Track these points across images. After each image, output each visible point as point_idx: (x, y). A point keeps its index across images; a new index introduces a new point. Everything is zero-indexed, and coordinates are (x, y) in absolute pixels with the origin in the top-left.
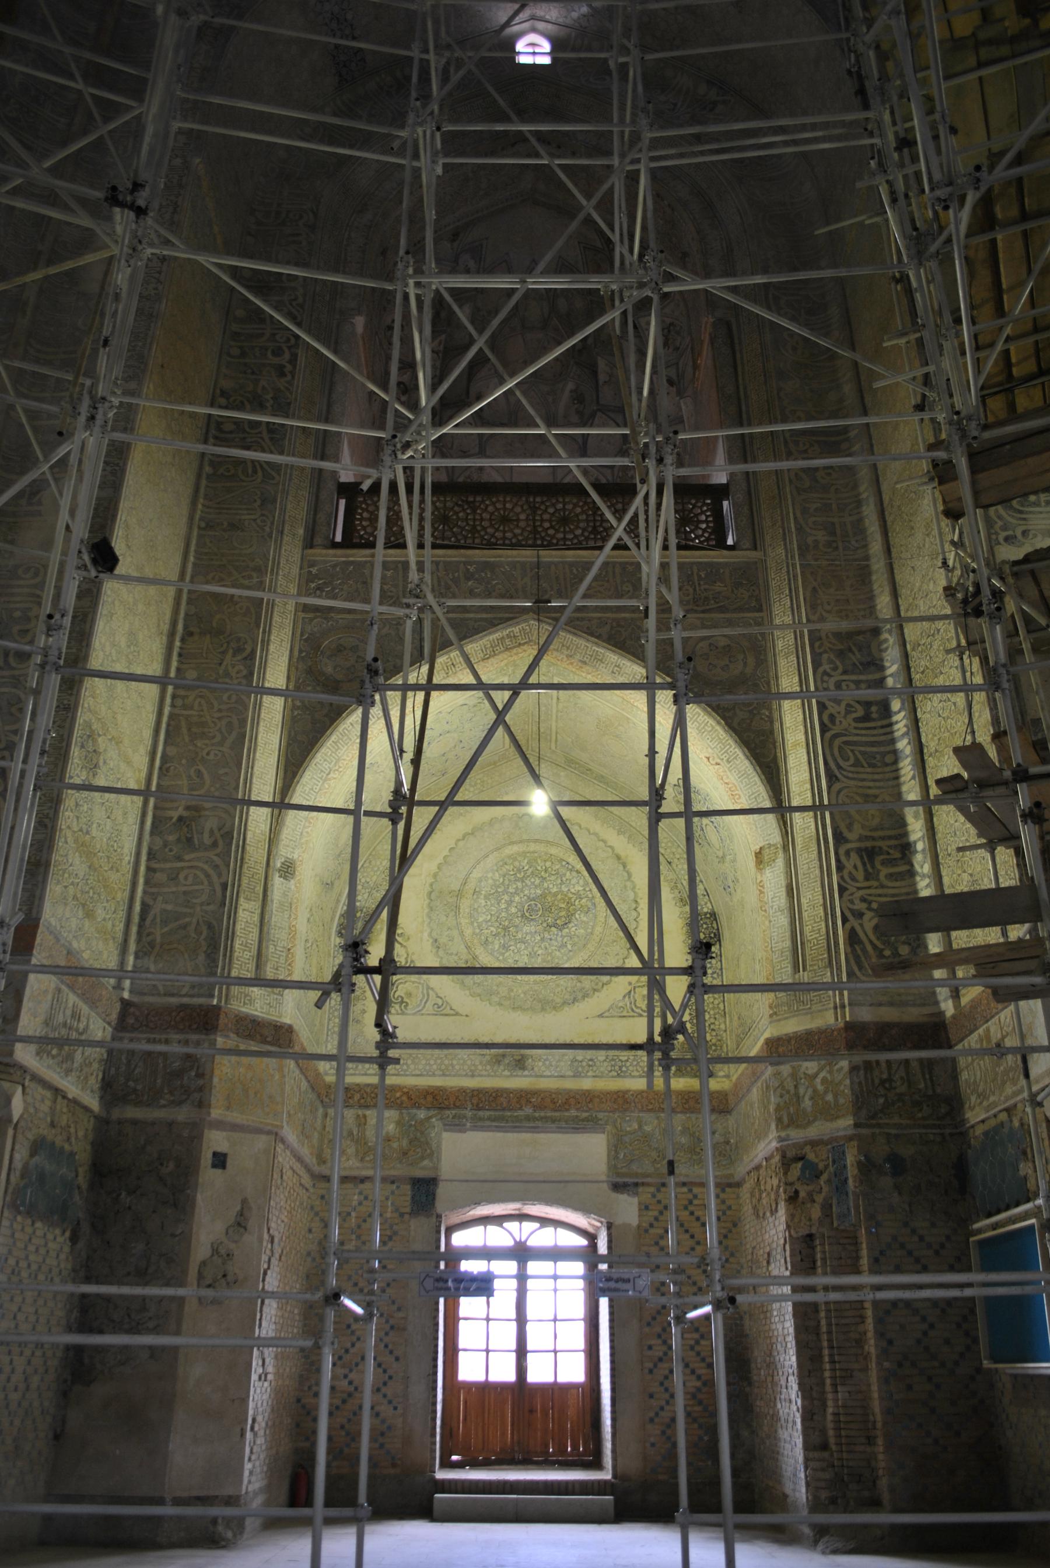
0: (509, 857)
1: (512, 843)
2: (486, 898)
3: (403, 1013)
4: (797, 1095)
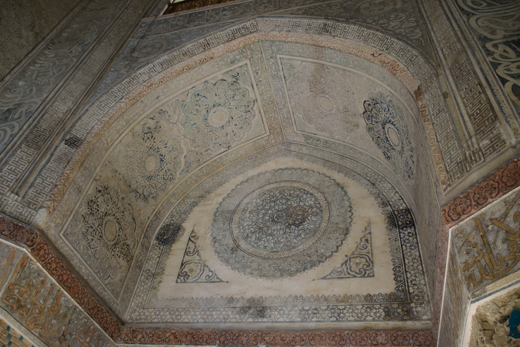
0: (268, 191)
1: (271, 184)
2: (250, 213)
3: (185, 282)
4: (486, 244)
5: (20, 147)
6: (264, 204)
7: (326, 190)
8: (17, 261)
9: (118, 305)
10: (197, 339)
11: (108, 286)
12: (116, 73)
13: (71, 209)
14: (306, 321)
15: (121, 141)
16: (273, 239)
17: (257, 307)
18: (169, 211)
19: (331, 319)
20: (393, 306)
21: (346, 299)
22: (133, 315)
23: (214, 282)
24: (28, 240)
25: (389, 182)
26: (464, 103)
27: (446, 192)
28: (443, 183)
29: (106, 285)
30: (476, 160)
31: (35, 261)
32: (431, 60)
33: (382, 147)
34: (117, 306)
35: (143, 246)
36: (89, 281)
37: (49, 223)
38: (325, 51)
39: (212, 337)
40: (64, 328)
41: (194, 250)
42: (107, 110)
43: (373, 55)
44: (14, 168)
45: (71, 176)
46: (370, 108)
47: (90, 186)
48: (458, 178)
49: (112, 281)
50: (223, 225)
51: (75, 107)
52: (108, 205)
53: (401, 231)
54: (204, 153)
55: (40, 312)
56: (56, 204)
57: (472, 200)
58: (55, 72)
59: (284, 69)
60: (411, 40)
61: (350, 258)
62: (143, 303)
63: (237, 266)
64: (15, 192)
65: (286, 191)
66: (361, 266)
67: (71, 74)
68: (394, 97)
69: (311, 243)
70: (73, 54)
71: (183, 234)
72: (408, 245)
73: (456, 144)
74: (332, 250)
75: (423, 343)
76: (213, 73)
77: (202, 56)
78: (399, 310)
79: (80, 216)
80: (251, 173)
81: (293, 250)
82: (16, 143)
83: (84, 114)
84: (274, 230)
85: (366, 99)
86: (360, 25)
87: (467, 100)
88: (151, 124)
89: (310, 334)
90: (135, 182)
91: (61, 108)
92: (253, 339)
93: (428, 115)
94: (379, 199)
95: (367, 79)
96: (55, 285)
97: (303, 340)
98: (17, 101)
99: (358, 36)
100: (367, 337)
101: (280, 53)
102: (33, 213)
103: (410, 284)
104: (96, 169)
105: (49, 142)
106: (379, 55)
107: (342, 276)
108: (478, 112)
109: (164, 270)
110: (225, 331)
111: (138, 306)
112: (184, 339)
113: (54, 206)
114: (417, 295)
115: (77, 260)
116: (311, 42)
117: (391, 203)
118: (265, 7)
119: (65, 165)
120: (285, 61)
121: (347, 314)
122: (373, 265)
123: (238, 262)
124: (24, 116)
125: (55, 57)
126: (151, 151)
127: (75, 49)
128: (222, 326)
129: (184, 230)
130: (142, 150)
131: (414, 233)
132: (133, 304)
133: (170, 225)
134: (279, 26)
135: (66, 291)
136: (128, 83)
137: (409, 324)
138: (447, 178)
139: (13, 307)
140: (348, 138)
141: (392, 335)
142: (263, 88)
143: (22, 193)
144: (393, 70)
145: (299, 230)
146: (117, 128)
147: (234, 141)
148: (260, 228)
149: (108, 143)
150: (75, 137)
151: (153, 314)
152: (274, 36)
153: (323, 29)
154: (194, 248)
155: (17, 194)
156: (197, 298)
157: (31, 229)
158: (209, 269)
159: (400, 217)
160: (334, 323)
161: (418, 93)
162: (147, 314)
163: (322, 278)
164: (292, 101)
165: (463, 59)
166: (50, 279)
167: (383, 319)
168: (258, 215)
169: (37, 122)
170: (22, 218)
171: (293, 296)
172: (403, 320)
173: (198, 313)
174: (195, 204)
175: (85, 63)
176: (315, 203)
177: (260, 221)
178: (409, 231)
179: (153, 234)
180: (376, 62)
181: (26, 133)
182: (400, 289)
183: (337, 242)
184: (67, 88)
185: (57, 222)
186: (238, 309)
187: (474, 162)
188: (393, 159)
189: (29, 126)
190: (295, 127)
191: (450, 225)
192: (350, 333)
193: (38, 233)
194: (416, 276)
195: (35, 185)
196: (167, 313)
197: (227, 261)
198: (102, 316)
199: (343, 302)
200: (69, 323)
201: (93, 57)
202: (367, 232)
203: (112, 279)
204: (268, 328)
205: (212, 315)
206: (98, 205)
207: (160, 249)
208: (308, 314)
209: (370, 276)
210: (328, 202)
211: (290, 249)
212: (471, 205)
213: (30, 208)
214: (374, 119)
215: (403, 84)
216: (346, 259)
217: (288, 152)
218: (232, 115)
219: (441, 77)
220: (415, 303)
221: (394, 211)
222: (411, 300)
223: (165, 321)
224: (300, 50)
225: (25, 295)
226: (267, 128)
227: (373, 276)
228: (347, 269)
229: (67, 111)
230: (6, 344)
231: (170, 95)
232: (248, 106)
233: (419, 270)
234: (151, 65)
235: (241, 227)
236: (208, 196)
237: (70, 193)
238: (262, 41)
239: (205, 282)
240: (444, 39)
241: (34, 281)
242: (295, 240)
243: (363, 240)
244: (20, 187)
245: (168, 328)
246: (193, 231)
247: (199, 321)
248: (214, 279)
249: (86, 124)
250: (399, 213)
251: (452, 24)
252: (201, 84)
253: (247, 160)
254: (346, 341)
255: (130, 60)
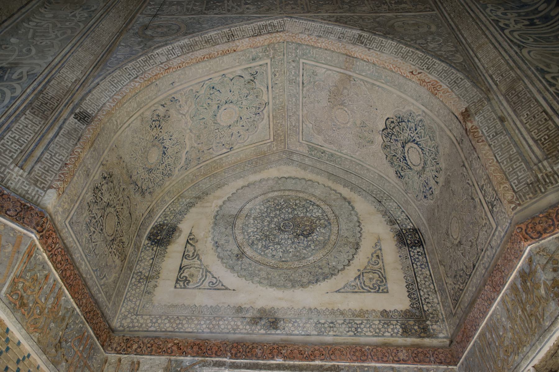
0: (272, 198)
1: (274, 191)
2: (254, 219)
3: (185, 288)
5: (23, 112)
6: (269, 211)
7: (333, 203)
8: (24, 249)
9: (109, 309)
10: (205, 350)
11: (103, 287)
12: (128, 49)
13: (78, 194)
14: (323, 335)
15: (129, 125)
16: (281, 248)
17: (268, 318)
18: (162, 209)
19: (349, 334)
20: (409, 322)
21: (362, 313)
22: (123, 322)
23: (218, 289)
24: (37, 225)
25: (394, 201)
26: (526, 128)
27: (515, 212)
28: (511, 202)
29: (101, 286)
30: (552, 183)
31: (42, 250)
32: (479, 85)
33: (395, 165)
34: (109, 313)
35: (135, 245)
36: (87, 280)
37: (57, 208)
38: (356, 62)
39: (222, 348)
40: (61, 333)
41: (194, 253)
42: (120, 87)
43: (412, 72)
44: (17, 137)
45: (82, 155)
46: (393, 125)
47: (97, 171)
48: (530, 198)
49: (106, 281)
50: (225, 230)
51: (84, 78)
52: (110, 195)
53: (410, 249)
54: (205, 152)
55: (41, 313)
56: (66, 186)
57: (555, 220)
58: (59, 35)
59: (305, 75)
60: (455, 63)
61: (363, 273)
62: (136, 309)
63: (244, 273)
64: (19, 165)
65: (291, 200)
66: (374, 282)
67: (79, 40)
68: (427, 117)
69: (321, 255)
70: (78, 18)
71: (179, 236)
72: (418, 264)
73: (524, 165)
74: (344, 264)
75: (443, 361)
76: (232, 67)
77: (225, 47)
78: (416, 327)
79: (85, 203)
80: (253, 178)
81: (303, 261)
82: (19, 108)
83: (94, 88)
84: (282, 239)
85: (392, 117)
86: (399, 41)
87: (530, 125)
88: (161, 111)
89: (329, 348)
90: (136, 173)
91: (69, 76)
92: (268, 351)
93: (482, 136)
94: (387, 217)
95: (398, 96)
96: (58, 282)
97: (323, 355)
98: (11, 59)
99: (396, 52)
100: (388, 353)
101: (305, 57)
102: (42, 193)
103: (424, 302)
104: (103, 152)
105: (57, 114)
106: (419, 73)
107: (356, 290)
108: (547, 137)
109: (159, 273)
110: (237, 343)
111: (129, 312)
112: (189, 350)
113: (63, 188)
114: (432, 313)
115: (79, 254)
116: (343, 51)
117: (399, 222)
118: (293, 8)
119: (74, 143)
120: (308, 67)
121: (365, 329)
122: (386, 281)
123: (245, 270)
124: (25, 78)
125: (54, 17)
126: (156, 142)
127: (79, 14)
128: (232, 337)
129: (181, 231)
130: (148, 139)
131: (423, 252)
132: (123, 310)
133: (164, 225)
134: (309, 30)
135: (67, 289)
136: (144, 62)
137: (427, 341)
138: (515, 197)
139: (16, 305)
140: (357, 154)
141: (413, 352)
142: (277, 91)
143: (28, 168)
144: (434, 90)
145: (308, 241)
146: (128, 110)
147: (238, 143)
148: (266, 236)
149: (117, 125)
150: (86, 112)
151: (149, 321)
152: (302, 39)
153: (357, 39)
154: (193, 251)
155: (21, 168)
156: (200, 306)
157: (41, 212)
158: (213, 275)
159: (408, 236)
160: (352, 338)
161: (466, 115)
162: (142, 321)
163: (336, 292)
164: (304, 109)
165: (520, 87)
166: (53, 274)
167: (401, 335)
168: (263, 222)
169: (42, 87)
170: (28, 198)
171: (307, 308)
172: (421, 337)
173: (202, 322)
174: (191, 205)
175: (93, 31)
176: (322, 215)
177: (266, 228)
178: (418, 250)
179: (145, 233)
180: (414, 80)
181: (30, 98)
182: (415, 306)
183: (349, 256)
184: (75, 54)
185: (65, 207)
186: (248, 320)
187: (550, 184)
188: (406, 179)
189: (34, 90)
190: (301, 136)
191: (529, 242)
192: (371, 349)
193: (49, 217)
194: (429, 295)
195: (42, 160)
196: (166, 321)
197: (232, 268)
198: (97, 322)
199: (359, 316)
200: (67, 328)
201: (101, 25)
202: (378, 248)
203: (107, 279)
204: (282, 340)
205: (219, 325)
206: (102, 194)
207: (153, 250)
208: (325, 328)
209: (384, 292)
210: (335, 216)
211: (300, 259)
212: (553, 225)
213: (37, 186)
214: (393, 137)
215: (445, 105)
216: (359, 273)
217: (290, 161)
218: (241, 115)
219: (493, 102)
220: (430, 321)
221: (402, 230)
222: (426, 317)
223: (163, 330)
224: (328, 58)
225: (28, 290)
226: (272, 133)
227: (387, 292)
228: (361, 283)
229: (76, 80)
230: (4, 350)
231: (186, 83)
232: (259, 108)
233: (431, 288)
234: (170, 47)
235: (246, 233)
236: (206, 198)
237: (79, 175)
238: (287, 42)
239: (208, 289)
240: (493, 66)
241: (38, 274)
242: (304, 251)
243: (374, 255)
244: (26, 160)
245: (169, 338)
246: (191, 233)
247: (205, 331)
248: (217, 286)
249: (97, 99)
250: (407, 232)
251: (500, 53)
252: (219, 76)
253: (247, 165)
254: (367, 356)
255: (143, 38)
